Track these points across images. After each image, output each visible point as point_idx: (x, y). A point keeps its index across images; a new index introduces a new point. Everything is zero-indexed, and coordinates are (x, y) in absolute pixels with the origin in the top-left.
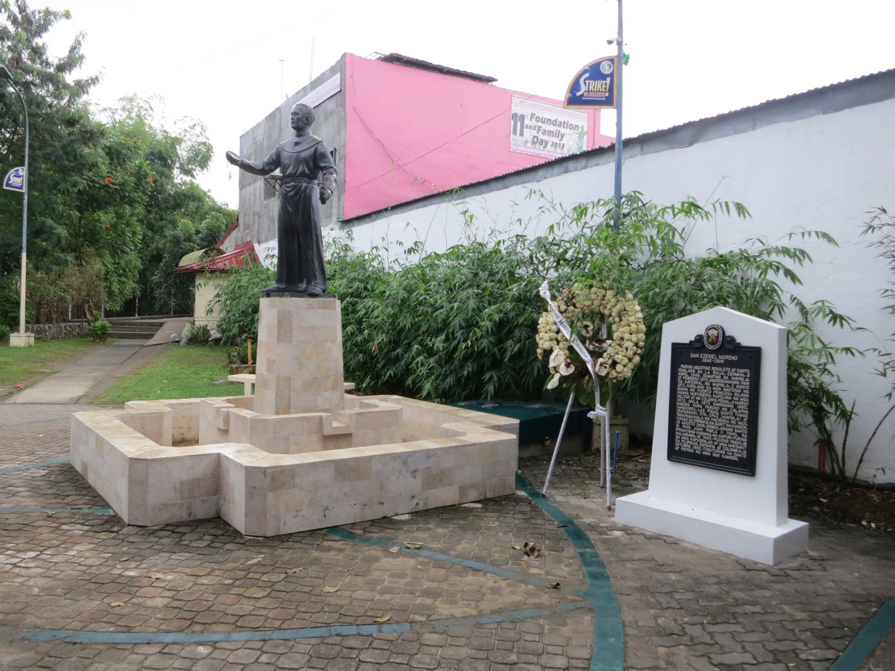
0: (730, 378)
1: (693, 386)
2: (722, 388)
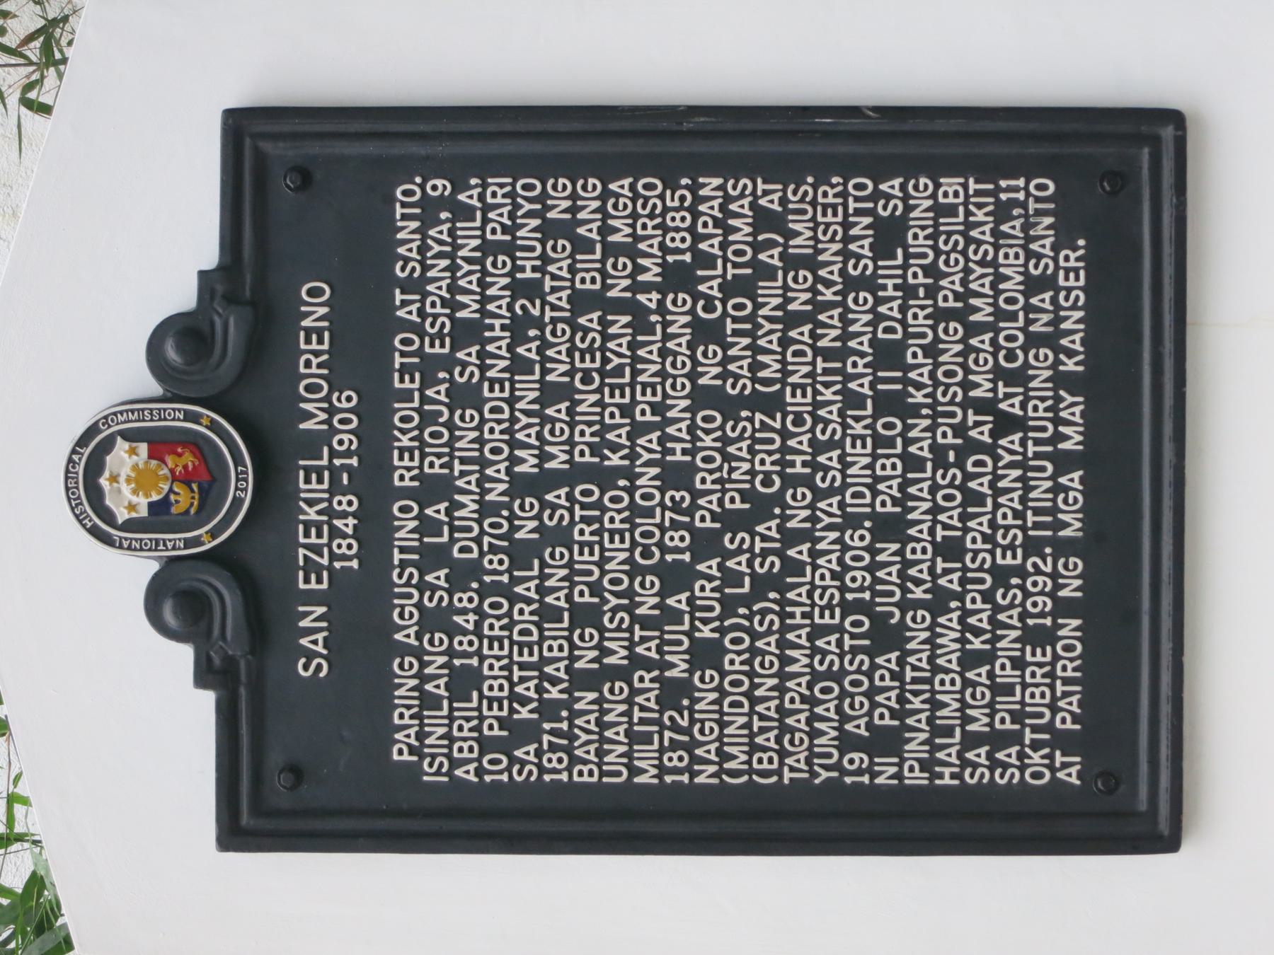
0: (467, 333)
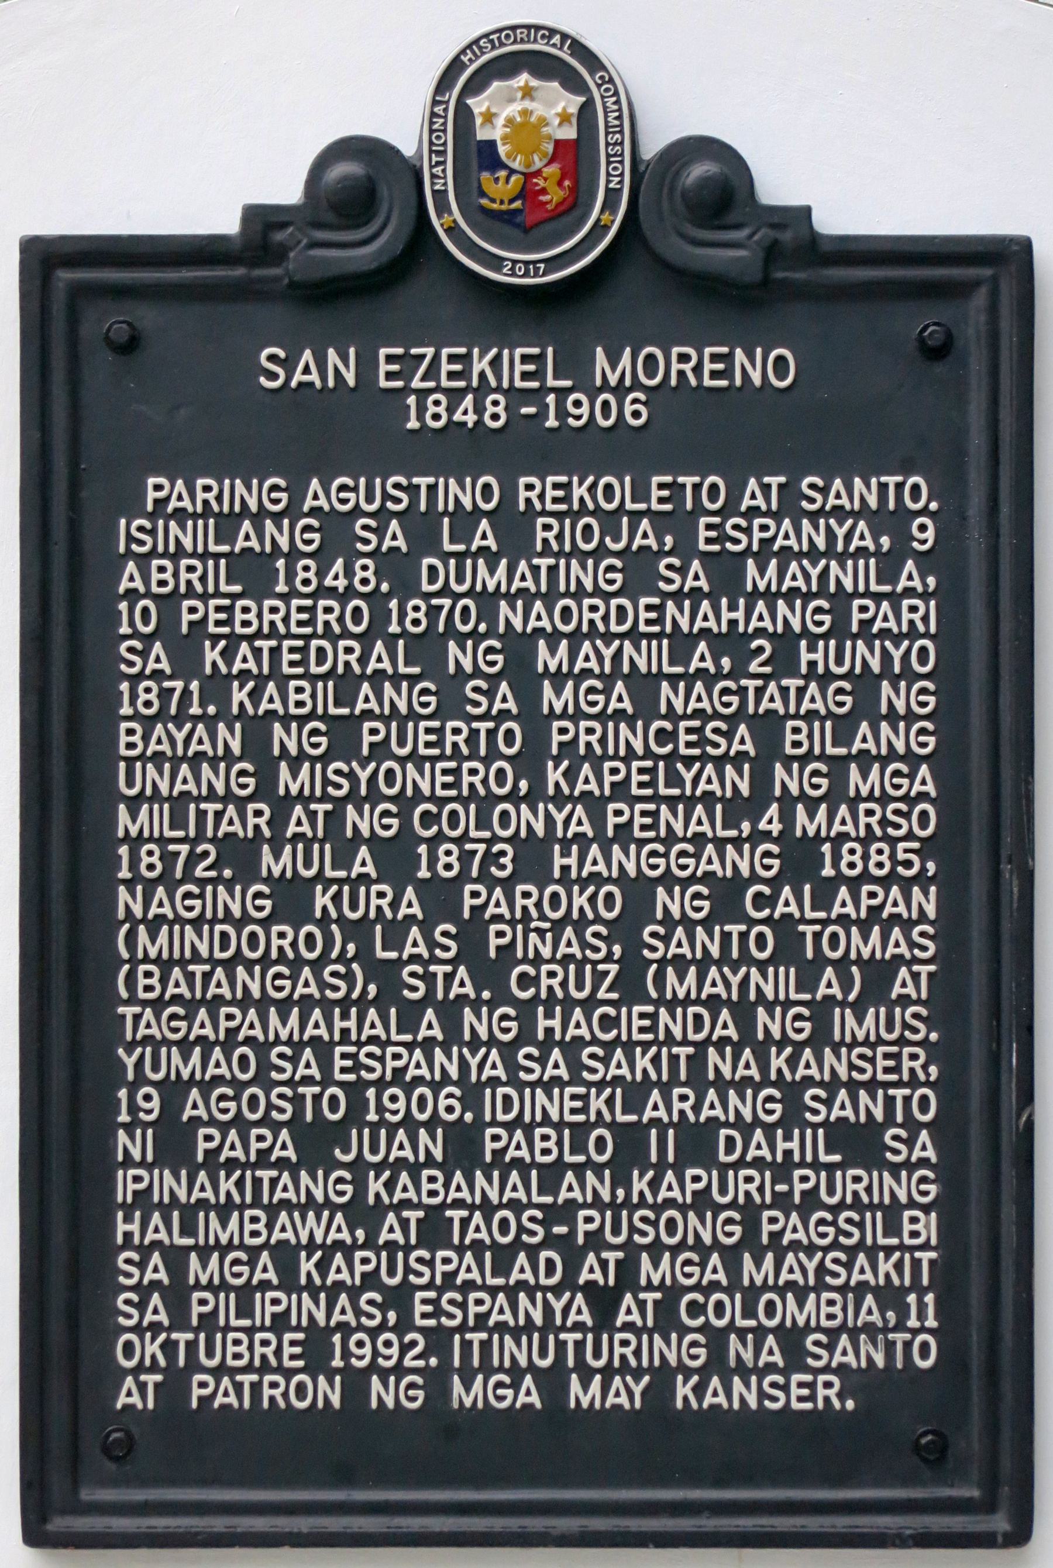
0: (726, 574)
1: (300, 696)
2: (645, 686)
